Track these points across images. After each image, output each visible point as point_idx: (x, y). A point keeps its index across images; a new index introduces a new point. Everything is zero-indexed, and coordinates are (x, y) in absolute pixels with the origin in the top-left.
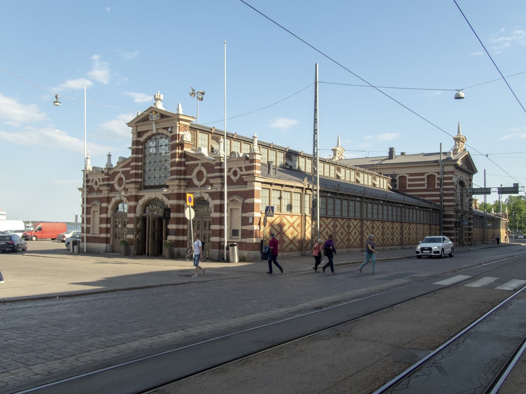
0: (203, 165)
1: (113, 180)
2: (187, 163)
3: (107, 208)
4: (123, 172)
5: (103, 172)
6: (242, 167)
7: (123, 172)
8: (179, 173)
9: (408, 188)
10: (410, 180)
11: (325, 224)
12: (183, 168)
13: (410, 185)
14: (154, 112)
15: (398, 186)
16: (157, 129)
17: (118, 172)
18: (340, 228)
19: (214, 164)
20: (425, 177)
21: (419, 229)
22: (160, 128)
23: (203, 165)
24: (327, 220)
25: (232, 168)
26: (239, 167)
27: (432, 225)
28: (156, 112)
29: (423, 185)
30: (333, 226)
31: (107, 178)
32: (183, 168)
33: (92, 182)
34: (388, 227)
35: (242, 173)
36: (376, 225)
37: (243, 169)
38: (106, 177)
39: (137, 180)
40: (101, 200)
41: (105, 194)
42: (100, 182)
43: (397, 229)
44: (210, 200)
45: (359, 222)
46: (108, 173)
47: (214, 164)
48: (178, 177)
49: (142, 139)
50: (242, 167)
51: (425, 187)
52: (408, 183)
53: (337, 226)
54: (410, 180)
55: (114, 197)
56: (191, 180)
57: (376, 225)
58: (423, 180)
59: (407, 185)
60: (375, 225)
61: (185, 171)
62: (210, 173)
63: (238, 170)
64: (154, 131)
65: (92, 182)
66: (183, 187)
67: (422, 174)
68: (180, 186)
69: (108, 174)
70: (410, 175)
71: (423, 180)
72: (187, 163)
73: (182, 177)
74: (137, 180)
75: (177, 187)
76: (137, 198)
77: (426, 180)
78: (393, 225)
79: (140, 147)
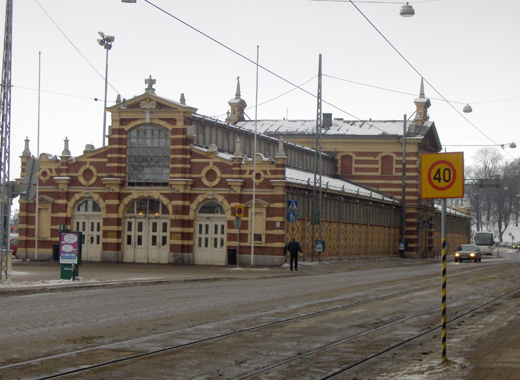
1: (77, 172)
2: (193, 160)
3: (66, 205)
4: (91, 163)
5: (57, 161)
6: (266, 171)
7: (91, 163)
8: (184, 171)
9: (354, 173)
10: (357, 162)
12: (188, 166)
13: (357, 170)
14: (148, 100)
15: (339, 170)
16: (151, 119)
17: (85, 163)
19: (232, 165)
20: (379, 158)
22: (156, 119)
23: (215, 164)
26: (262, 171)
28: (151, 100)
29: (376, 170)
31: (67, 169)
32: (188, 166)
35: (266, 176)
37: (268, 172)
38: (65, 167)
39: (119, 175)
40: (56, 195)
42: (51, 172)
44: (226, 203)
46: (67, 163)
47: (232, 165)
48: (184, 175)
49: (126, 128)
50: (266, 171)
51: (378, 174)
52: (354, 165)
54: (357, 162)
55: (78, 192)
56: (199, 179)
58: (376, 162)
59: (353, 170)
61: (190, 168)
62: (224, 174)
63: (261, 173)
64: (148, 121)
66: (189, 187)
67: (375, 154)
68: (185, 185)
69: (67, 164)
70: (358, 154)
71: (376, 162)
72: (193, 160)
73: (188, 175)
74: (119, 175)
75: (182, 187)
76: (120, 196)
77: (380, 162)
79: (124, 136)
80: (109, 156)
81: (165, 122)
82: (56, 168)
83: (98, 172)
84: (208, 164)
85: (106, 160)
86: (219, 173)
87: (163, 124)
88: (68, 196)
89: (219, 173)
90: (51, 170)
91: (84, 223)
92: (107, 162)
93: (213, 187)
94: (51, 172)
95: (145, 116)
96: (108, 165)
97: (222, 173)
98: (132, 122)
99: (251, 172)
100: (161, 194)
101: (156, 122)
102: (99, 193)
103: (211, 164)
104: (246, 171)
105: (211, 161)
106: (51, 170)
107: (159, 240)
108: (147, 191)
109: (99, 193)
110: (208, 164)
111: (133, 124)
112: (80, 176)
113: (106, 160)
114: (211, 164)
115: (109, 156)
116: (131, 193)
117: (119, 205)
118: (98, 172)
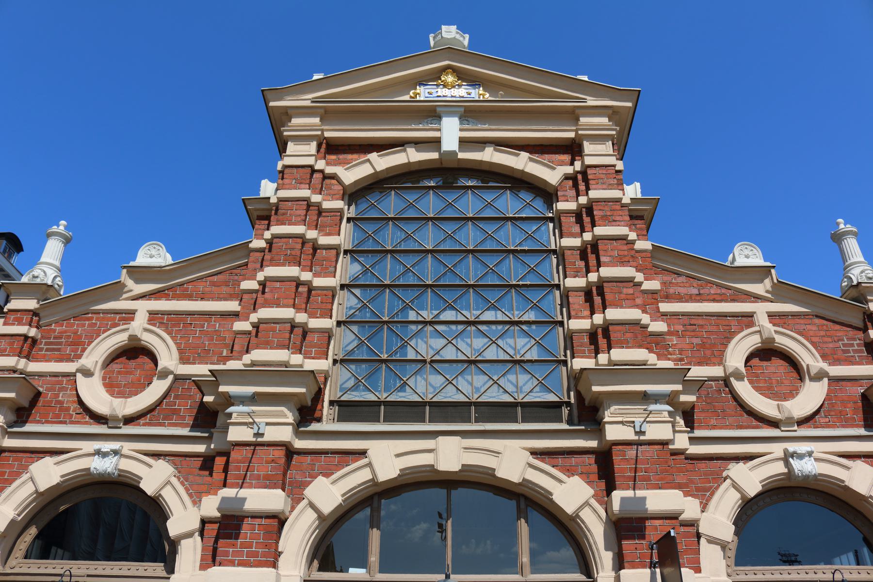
7: (154, 317)
14: (450, 79)
81: (525, 155)
83: (184, 359)
84: (748, 319)
93: (803, 422)
101: (489, 155)
103: (763, 320)
105: (761, 310)
108: (457, 439)
110: (748, 319)
112: (87, 373)
114: (763, 320)
116: (363, 453)
117: (279, 520)
118: (184, 359)
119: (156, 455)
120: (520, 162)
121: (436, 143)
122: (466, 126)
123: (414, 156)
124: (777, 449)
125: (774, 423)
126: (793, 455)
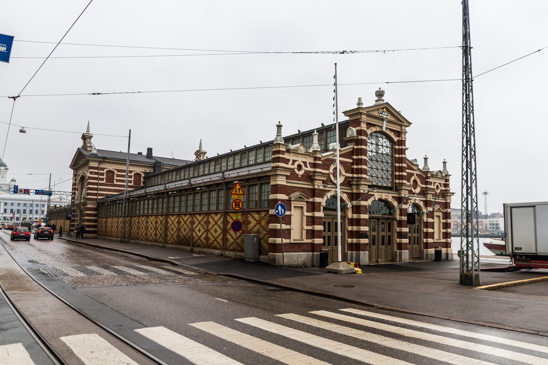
0: (417, 175)
11: (214, 220)
14: (385, 110)
18: (198, 225)
21: (153, 222)
23: (417, 175)
24: (200, 216)
25: (435, 183)
27: (127, 218)
30: (194, 223)
33: (293, 164)
34: (143, 222)
36: (171, 220)
41: (319, 185)
42: (306, 166)
43: (151, 222)
45: (189, 217)
47: (425, 177)
53: (190, 223)
57: (171, 220)
60: (158, 220)
63: (439, 185)
65: (293, 164)
78: (139, 219)
80: (355, 157)
81: (393, 133)
82: (310, 162)
84: (413, 174)
85: (350, 161)
86: (419, 183)
87: (392, 135)
88: (322, 193)
89: (419, 183)
90: (305, 163)
91: (329, 223)
92: (352, 164)
94: (306, 166)
95: (383, 124)
96: (355, 167)
97: (421, 184)
98: (372, 128)
99: (435, 183)
100: (393, 197)
101: (388, 132)
102: (346, 193)
104: (432, 182)
105: (415, 172)
106: (305, 163)
107: (386, 240)
109: (347, 193)
111: (374, 129)
113: (350, 161)
115: (355, 157)
116: (373, 195)
119: (344, 192)
120: (392, 135)
121: (381, 127)
122: (388, 124)
123: (378, 129)
124: (414, 198)
125: (414, 194)
126: (416, 200)
